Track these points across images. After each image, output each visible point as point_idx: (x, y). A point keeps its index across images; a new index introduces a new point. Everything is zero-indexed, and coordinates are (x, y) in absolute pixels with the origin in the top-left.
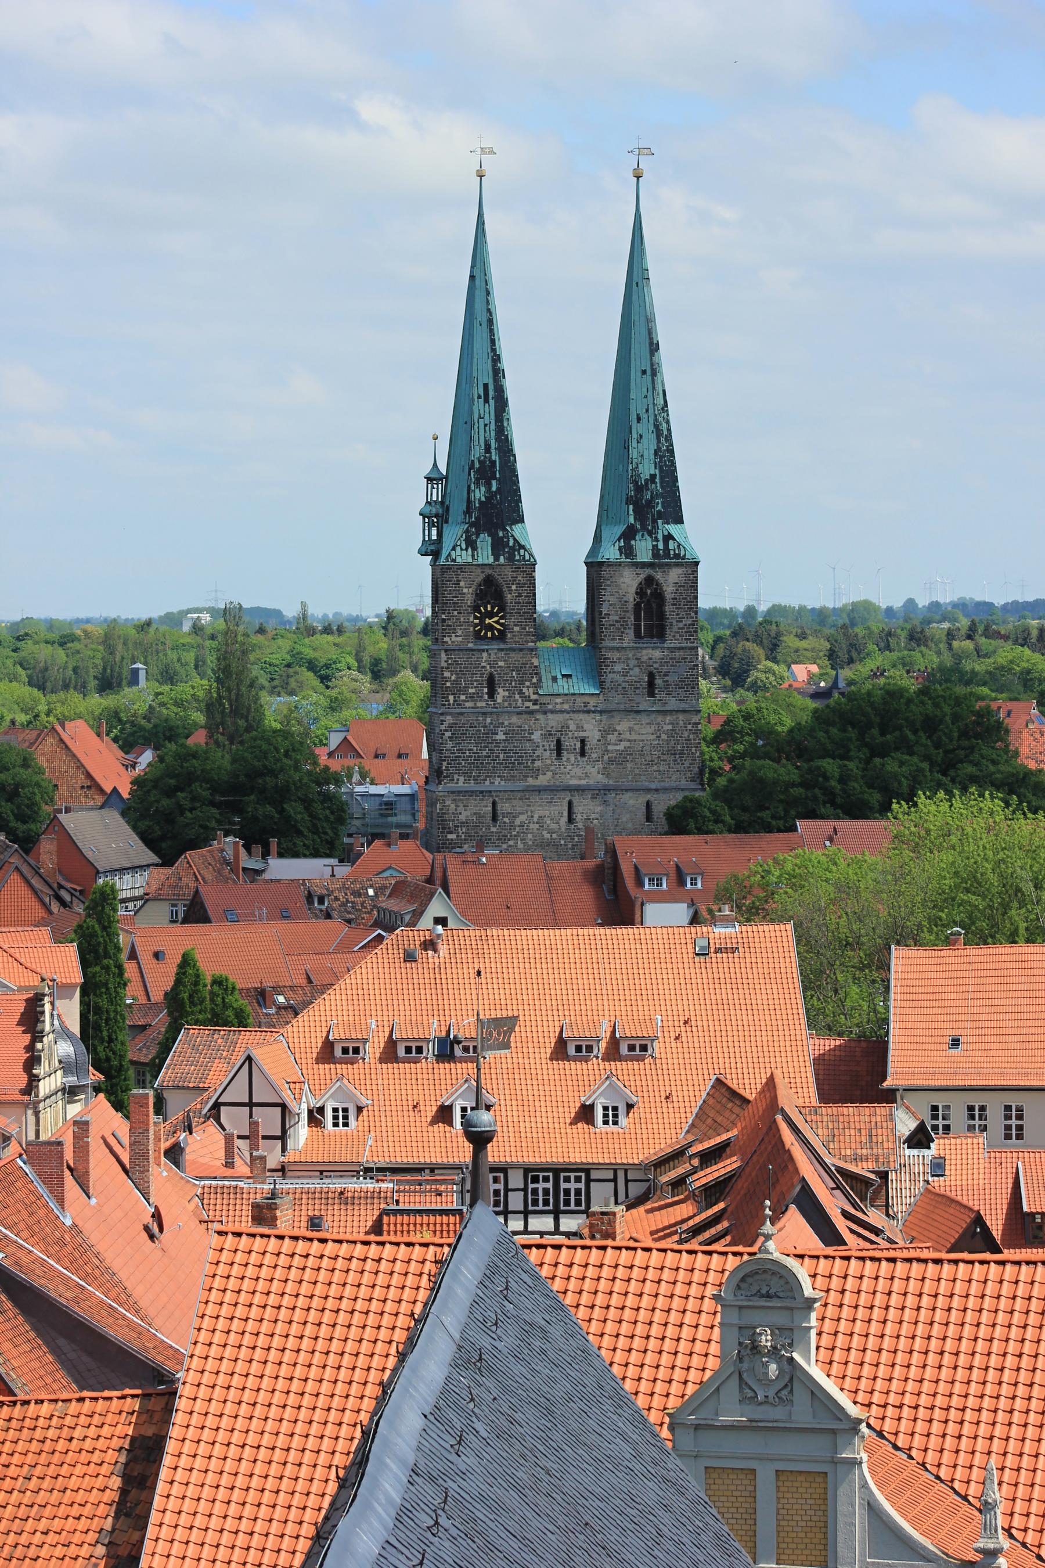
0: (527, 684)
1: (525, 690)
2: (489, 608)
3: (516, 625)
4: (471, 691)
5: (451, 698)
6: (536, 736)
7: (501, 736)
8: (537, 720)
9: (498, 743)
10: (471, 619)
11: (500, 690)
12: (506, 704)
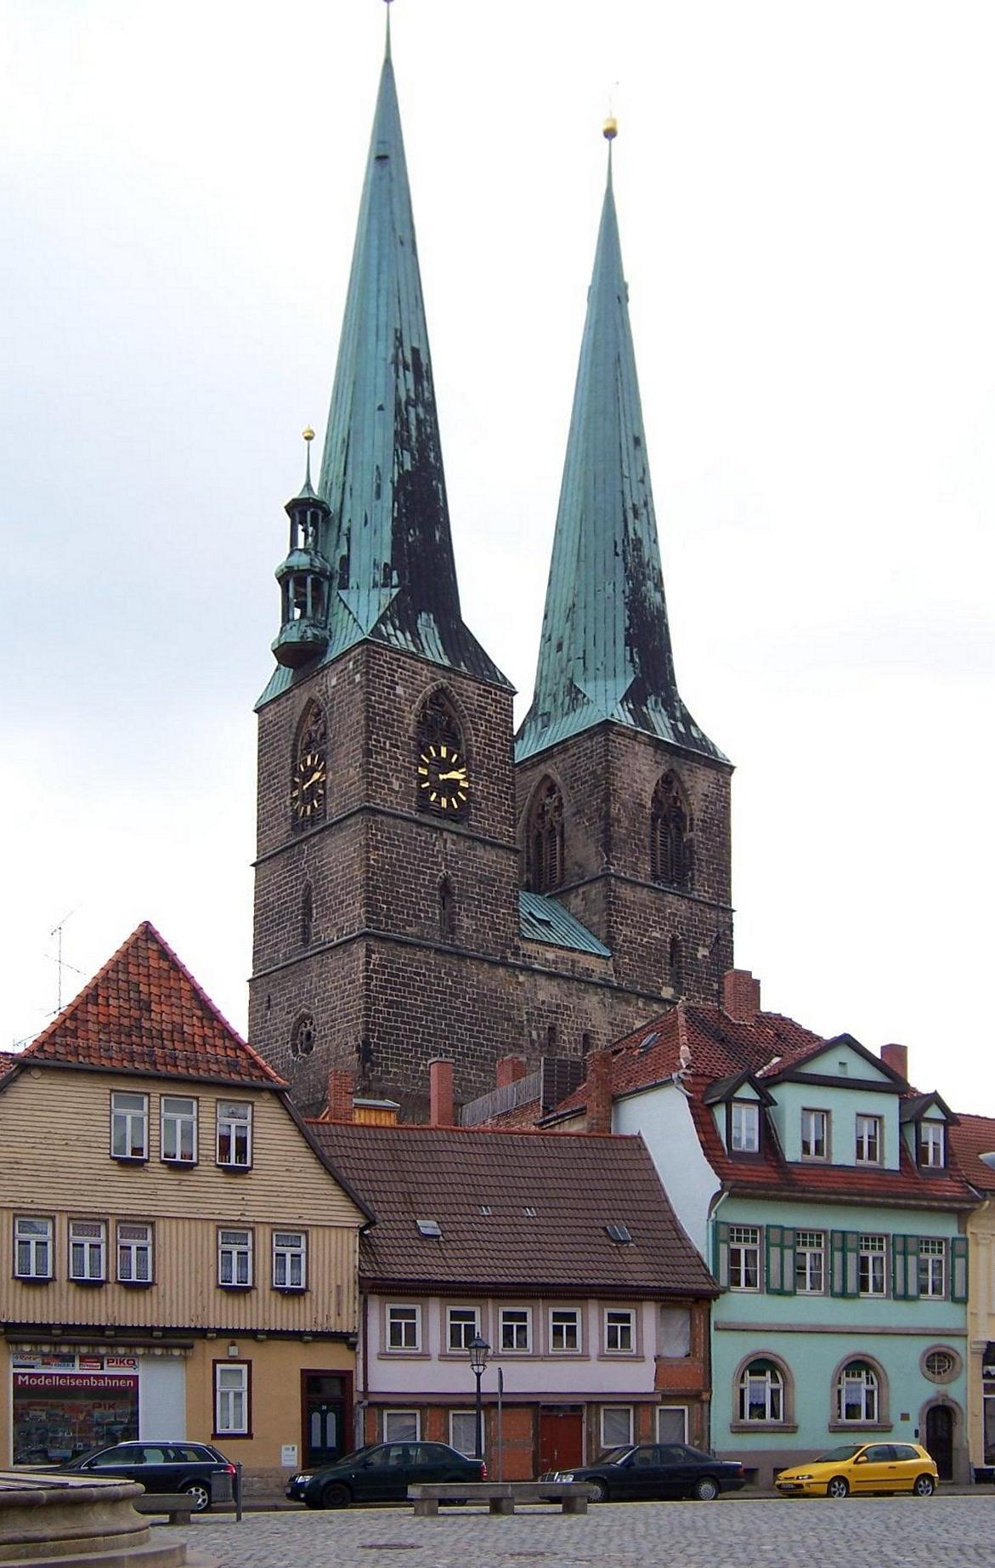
2: (444, 753)
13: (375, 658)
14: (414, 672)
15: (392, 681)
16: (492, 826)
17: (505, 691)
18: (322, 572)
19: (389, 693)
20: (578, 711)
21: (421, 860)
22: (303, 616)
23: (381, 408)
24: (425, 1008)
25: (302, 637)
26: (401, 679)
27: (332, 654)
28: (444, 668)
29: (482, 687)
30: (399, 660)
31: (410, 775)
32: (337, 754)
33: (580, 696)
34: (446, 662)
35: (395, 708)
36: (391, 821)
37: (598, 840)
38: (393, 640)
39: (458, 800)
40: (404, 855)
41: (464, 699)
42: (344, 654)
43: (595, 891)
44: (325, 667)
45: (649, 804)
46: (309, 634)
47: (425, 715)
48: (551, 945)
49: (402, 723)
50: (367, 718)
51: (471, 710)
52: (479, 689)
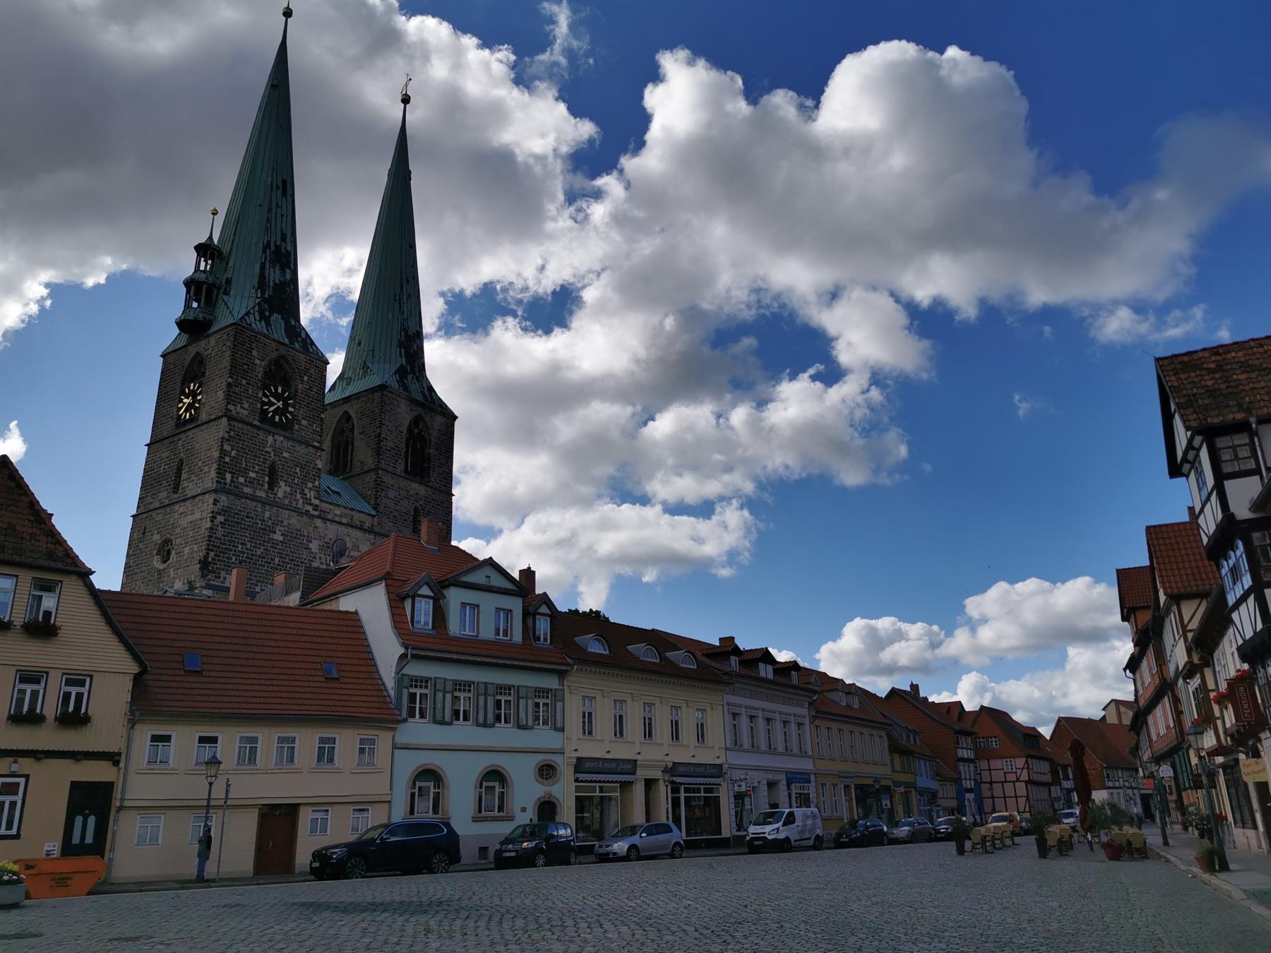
0: (310, 485)
1: (307, 491)
2: (280, 390)
3: (304, 419)
4: (252, 475)
5: (228, 476)
6: (314, 546)
7: (278, 537)
8: (316, 527)
9: (275, 544)
10: (260, 395)
11: (282, 484)
12: (287, 502)
17: (323, 361)
18: (213, 285)
21: (258, 450)
22: (199, 306)
23: (260, 205)
27: (213, 330)
28: (286, 345)
34: (287, 341)
36: (240, 425)
38: (254, 326)
39: (286, 417)
40: (247, 446)
42: (221, 329)
43: (370, 478)
44: (209, 336)
45: (405, 432)
46: (201, 316)
47: (270, 369)
48: (339, 506)
50: (231, 366)
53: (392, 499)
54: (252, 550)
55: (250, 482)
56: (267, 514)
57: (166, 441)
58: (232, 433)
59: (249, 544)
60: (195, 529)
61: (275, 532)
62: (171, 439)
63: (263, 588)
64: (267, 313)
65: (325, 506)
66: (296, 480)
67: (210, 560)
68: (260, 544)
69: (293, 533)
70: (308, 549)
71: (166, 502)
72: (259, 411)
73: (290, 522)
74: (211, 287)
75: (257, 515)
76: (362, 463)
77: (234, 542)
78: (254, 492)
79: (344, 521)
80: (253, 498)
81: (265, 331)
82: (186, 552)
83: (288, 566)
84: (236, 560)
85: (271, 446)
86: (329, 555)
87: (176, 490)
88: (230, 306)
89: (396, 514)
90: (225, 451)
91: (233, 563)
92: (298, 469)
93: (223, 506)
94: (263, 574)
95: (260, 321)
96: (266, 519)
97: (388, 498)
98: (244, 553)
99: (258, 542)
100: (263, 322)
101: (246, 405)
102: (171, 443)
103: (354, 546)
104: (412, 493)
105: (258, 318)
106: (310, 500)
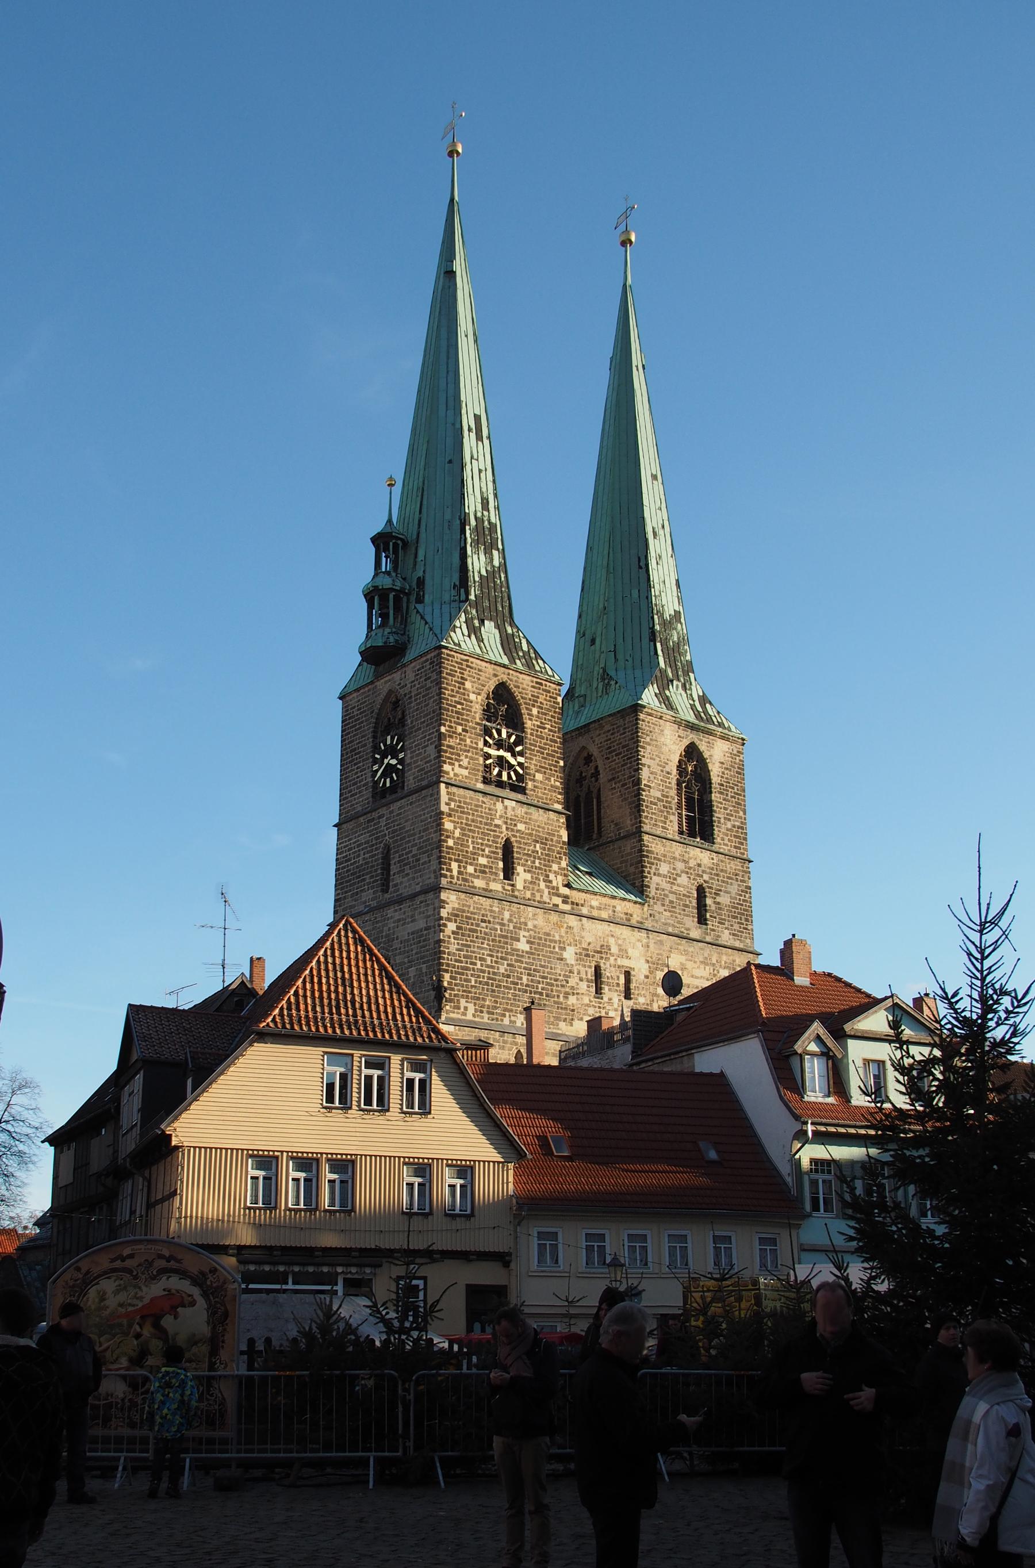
0: (555, 867)
1: (552, 877)
2: (504, 735)
4: (483, 861)
7: (523, 946)
9: (520, 955)
10: (481, 744)
11: (520, 869)
13: (448, 660)
14: (480, 670)
15: (462, 678)
16: (544, 794)
18: (402, 591)
19: (459, 688)
20: (611, 694)
21: (486, 824)
24: (490, 950)
25: (385, 643)
26: (469, 676)
28: (504, 666)
29: (535, 680)
30: (467, 661)
31: (477, 754)
32: (416, 736)
33: (613, 683)
35: (465, 699)
36: (461, 791)
37: (630, 803)
38: (462, 644)
41: (520, 690)
46: (392, 639)
48: (595, 893)
49: (471, 711)
51: (525, 699)
52: (532, 682)
53: (665, 876)
54: (493, 967)
55: (482, 871)
56: (507, 915)
57: (361, 819)
58: (453, 804)
59: (489, 958)
60: (420, 942)
61: (518, 940)
62: (369, 817)
63: (513, 1018)
64: (476, 623)
65: (576, 896)
66: (537, 861)
67: (445, 984)
68: (502, 958)
69: (540, 939)
70: (562, 959)
71: (374, 904)
72: (481, 769)
73: (536, 922)
74: (400, 595)
75: (494, 918)
76: (616, 825)
77: (470, 957)
78: (487, 884)
79: (604, 915)
80: (487, 894)
81: (478, 651)
82: (411, 975)
83: (540, 986)
84: (476, 982)
85: (501, 817)
86: (590, 967)
87: (385, 889)
88: (428, 618)
89: (672, 897)
90: (447, 831)
91: (472, 986)
92: (538, 845)
93: (453, 909)
94: (510, 999)
95: (469, 636)
96: (505, 922)
97: (659, 875)
98: (483, 972)
99: (500, 955)
100: (473, 637)
101: (465, 762)
102: (369, 821)
103: (620, 950)
104: (692, 863)
105: (466, 633)
106: (558, 889)
